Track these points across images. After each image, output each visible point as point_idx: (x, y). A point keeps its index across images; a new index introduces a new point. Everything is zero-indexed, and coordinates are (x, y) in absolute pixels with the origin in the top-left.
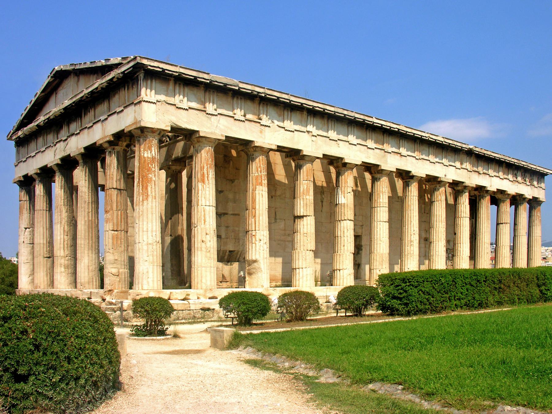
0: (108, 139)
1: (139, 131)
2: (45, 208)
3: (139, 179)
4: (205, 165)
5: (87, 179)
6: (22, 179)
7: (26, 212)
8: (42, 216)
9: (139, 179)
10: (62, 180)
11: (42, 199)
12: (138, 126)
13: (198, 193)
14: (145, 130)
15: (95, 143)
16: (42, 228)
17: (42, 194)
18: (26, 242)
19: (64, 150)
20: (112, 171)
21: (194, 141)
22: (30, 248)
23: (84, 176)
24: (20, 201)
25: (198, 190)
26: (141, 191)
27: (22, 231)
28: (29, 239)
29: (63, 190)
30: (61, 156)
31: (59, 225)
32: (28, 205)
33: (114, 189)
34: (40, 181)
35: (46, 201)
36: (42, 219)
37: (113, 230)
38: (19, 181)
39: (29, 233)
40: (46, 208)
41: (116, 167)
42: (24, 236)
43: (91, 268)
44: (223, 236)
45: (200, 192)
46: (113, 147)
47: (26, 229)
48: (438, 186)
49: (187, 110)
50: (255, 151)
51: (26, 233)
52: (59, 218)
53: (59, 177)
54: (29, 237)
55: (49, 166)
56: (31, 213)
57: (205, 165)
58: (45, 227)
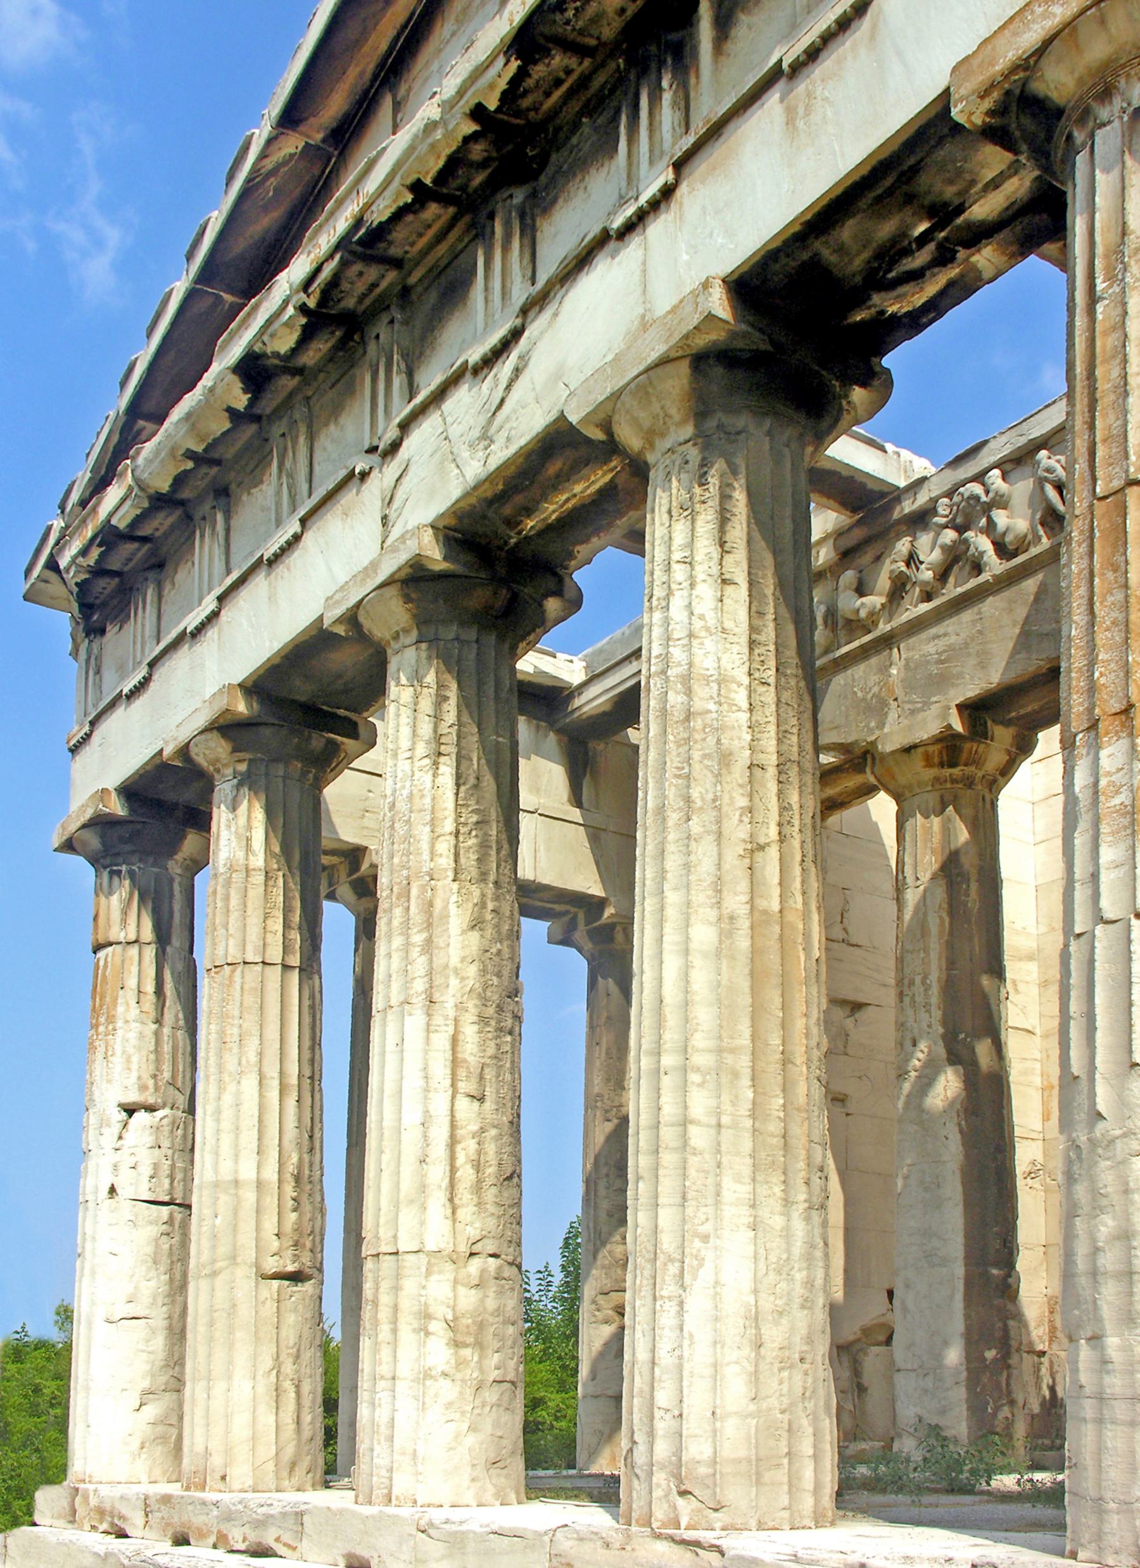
5: (741, 576)
8: (251, 1000)
11: (256, 891)
16: (250, 1084)
18: (125, 1191)
22: (154, 1231)
23: (706, 546)
24: (97, 948)
27: (103, 1123)
28: (146, 1170)
32: (151, 972)
34: (247, 781)
35: (287, 910)
36: (250, 1023)
38: (100, 823)
39: (149, 1140)
42: (121, 1158)
43: (774, 1335)
47: (130, 1111)
53: (417, 678)
54: (146, 1159)
56: (169, 1017)
58: (272, 1071)
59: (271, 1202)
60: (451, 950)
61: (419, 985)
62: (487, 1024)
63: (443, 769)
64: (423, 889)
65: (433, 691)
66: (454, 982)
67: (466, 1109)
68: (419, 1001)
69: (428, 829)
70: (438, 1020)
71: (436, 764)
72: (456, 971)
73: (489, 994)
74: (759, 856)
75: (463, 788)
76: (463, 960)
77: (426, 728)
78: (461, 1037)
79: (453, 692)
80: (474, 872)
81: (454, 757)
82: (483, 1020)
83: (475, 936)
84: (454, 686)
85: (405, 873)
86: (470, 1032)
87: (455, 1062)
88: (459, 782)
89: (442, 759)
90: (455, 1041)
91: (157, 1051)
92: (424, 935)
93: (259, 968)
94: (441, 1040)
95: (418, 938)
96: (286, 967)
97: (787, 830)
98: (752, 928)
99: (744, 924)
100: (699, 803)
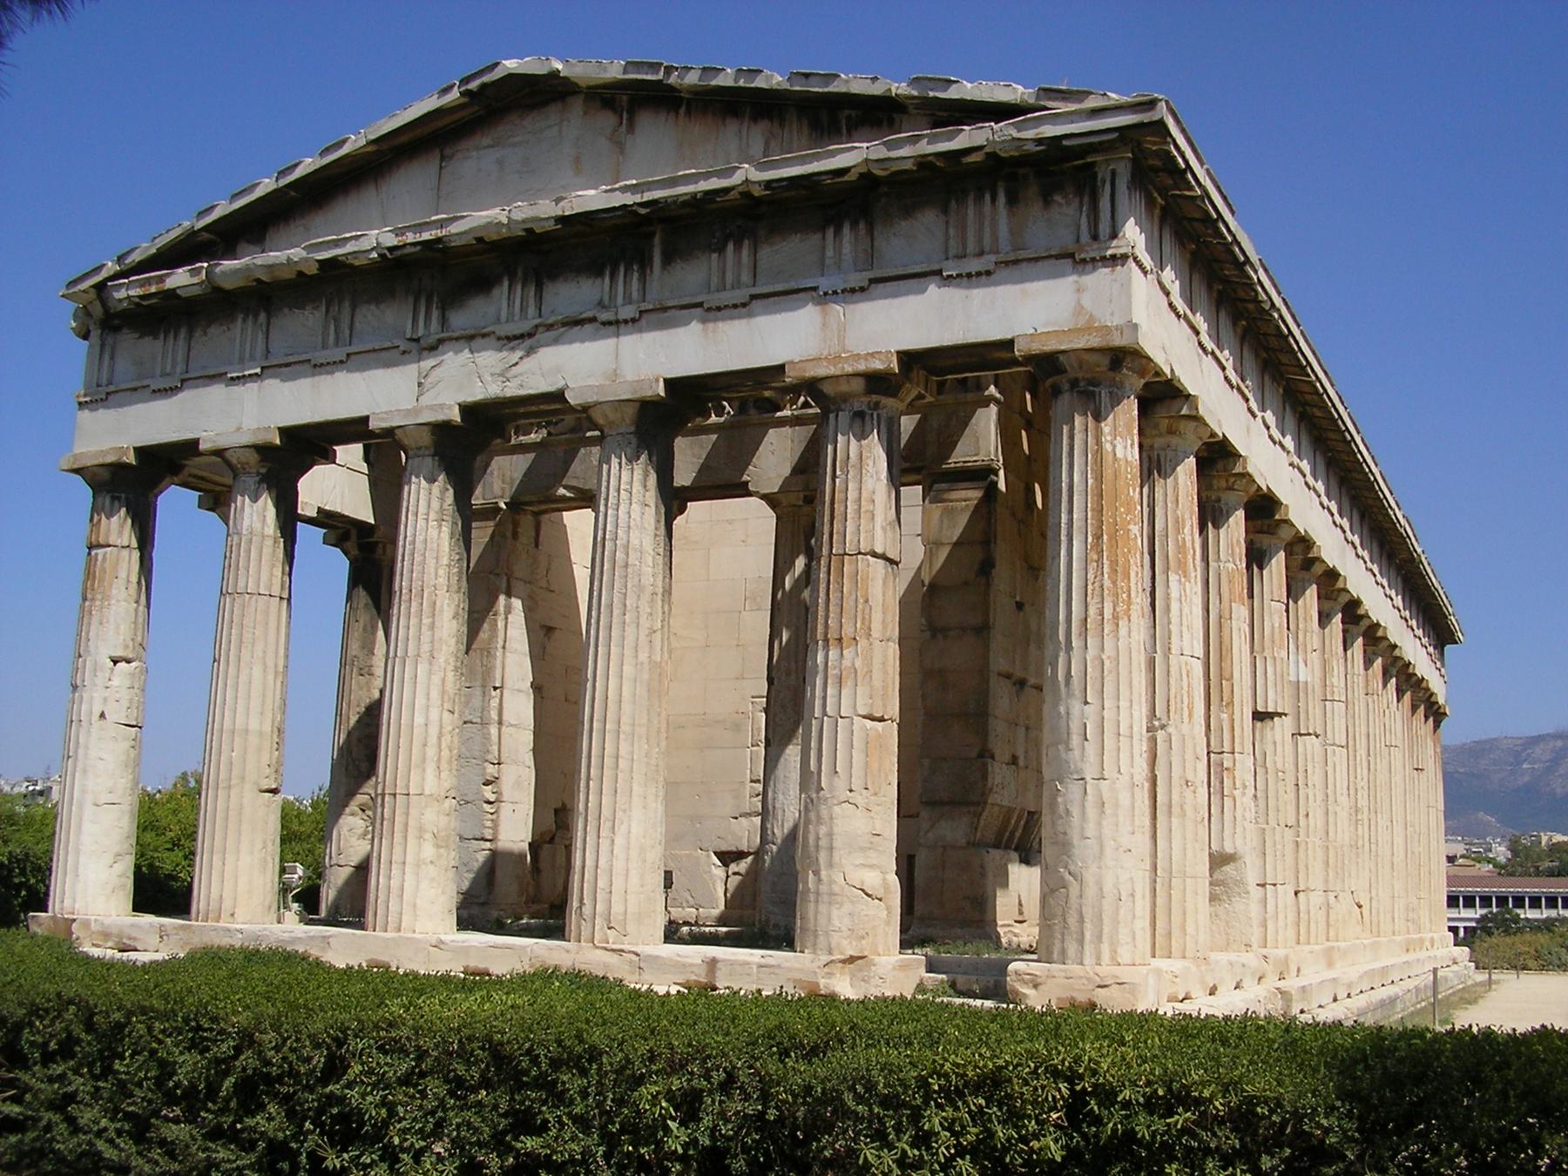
0: (878, 365)
1: (1105, 361)
2: (276, 591)
3: (1098, 537)
4: (1187, 516)
6: (131, 459)
7: (123, 594)
9: (1098, 537)
12: (1118, 341)
13: (1168, 609)
14: (1128, 362)
15: (780, 369)
19: (503, 375)
20: (869, 484)
21: (1156, 426)
22: (127, 744)
25: (1168, 597)
26: (1107, 583)
30: (476, 394)
33: (875, 555)
37: (873, 719)
41: (884, 474)
44: (1021, 763)
45: (1174, 606)
46: (875, 398)
47: (115, 662)
48: (1370, 649)
49: (1179, 317)
50: (1231, 489)
51: (116, 682)
54: (125, 696)
55: (373, 425)
57: (1187, 516)
59: (267, 744)
61: (426, 647)
64: (430, 594)
67: (446, 715)
68: (425, 655)
70: (435, 668)
77: (435, 504)
82: (456, 669)
86: (450, 675)
87: (443, 692)
90: (443, 680)
91: (135, 623)
94: (436, 679)
99: (647, 667)
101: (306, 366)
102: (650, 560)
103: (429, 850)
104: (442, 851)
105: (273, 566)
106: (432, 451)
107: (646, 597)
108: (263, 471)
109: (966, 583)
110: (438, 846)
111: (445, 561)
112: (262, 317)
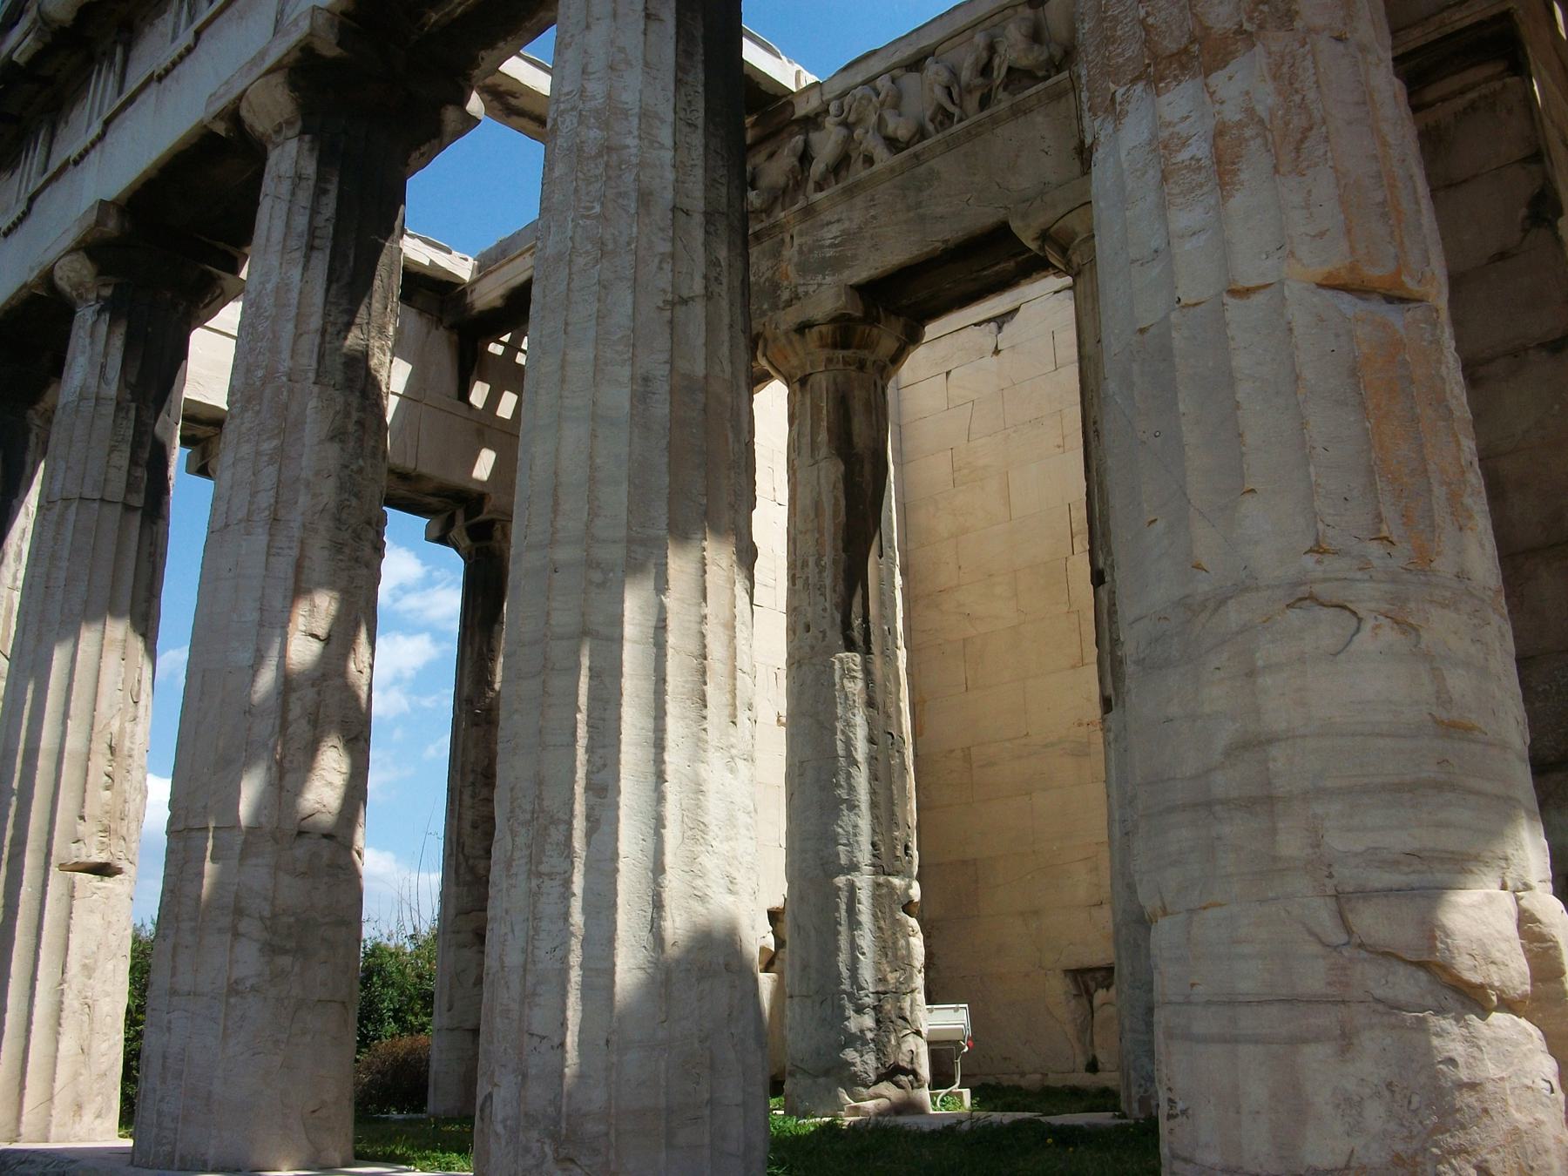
2: (117, 488)
10: (320, 192)
17: (112, 390)
29: (321, 262)
31: (261, 538)
37: (1359, 289)
40: (130, 487)
52: (269, 475)
60: (304, 463)
61: (265, 499)
62: (340, 551)
63: (313, 262)
65: (311, 183)
66: (303, 499)
69: (290, 326)
71: (307, 258)
72: (308, 485)
73: (344, 516)
74: (680, 311)
75: (334, 286)
76: (317, 473)
77: (301, 222)
78: (307, 563)
79: (333, 189)
80: (339, 377)
81: (328, 252)
82: (337, 547)
83: (333, 450)
84: (335, 180)
85: (260, 373)
88: (330, 281)
89: (315, 254)
92: (275, 442)
93: (96, 505)
95: (267, 446)
96: (128, 508)
97: (715, 288)
98: (671, 392)
99: (662, 388)
100: (610, 247)
101: (154, 85)
102: (665, 135)
103: (249, 961)
104: (285, 961)
105: (113, 449)
106: (299, 125)
107: (661, 211)
108: (107, 292)
109: (1502, 256)
110: (271, 950)
111: (315, 322)
112: (119, 51)
